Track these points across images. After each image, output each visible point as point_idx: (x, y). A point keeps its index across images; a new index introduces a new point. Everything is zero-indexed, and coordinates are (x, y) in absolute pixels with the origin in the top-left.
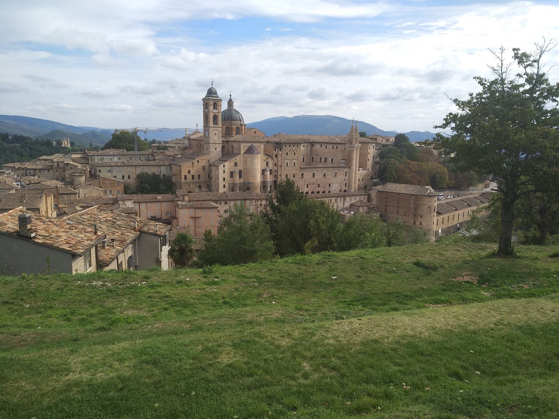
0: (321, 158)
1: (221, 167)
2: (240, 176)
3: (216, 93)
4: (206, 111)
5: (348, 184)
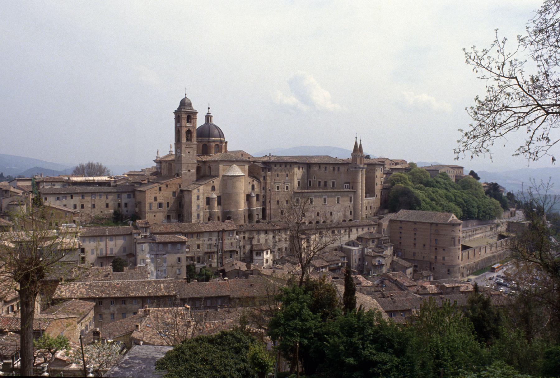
0: (320, 182)
1: (195, 191)
2: (219, 203)
3: (190, 104)
4: (178, 125)
5: (354, 212)
